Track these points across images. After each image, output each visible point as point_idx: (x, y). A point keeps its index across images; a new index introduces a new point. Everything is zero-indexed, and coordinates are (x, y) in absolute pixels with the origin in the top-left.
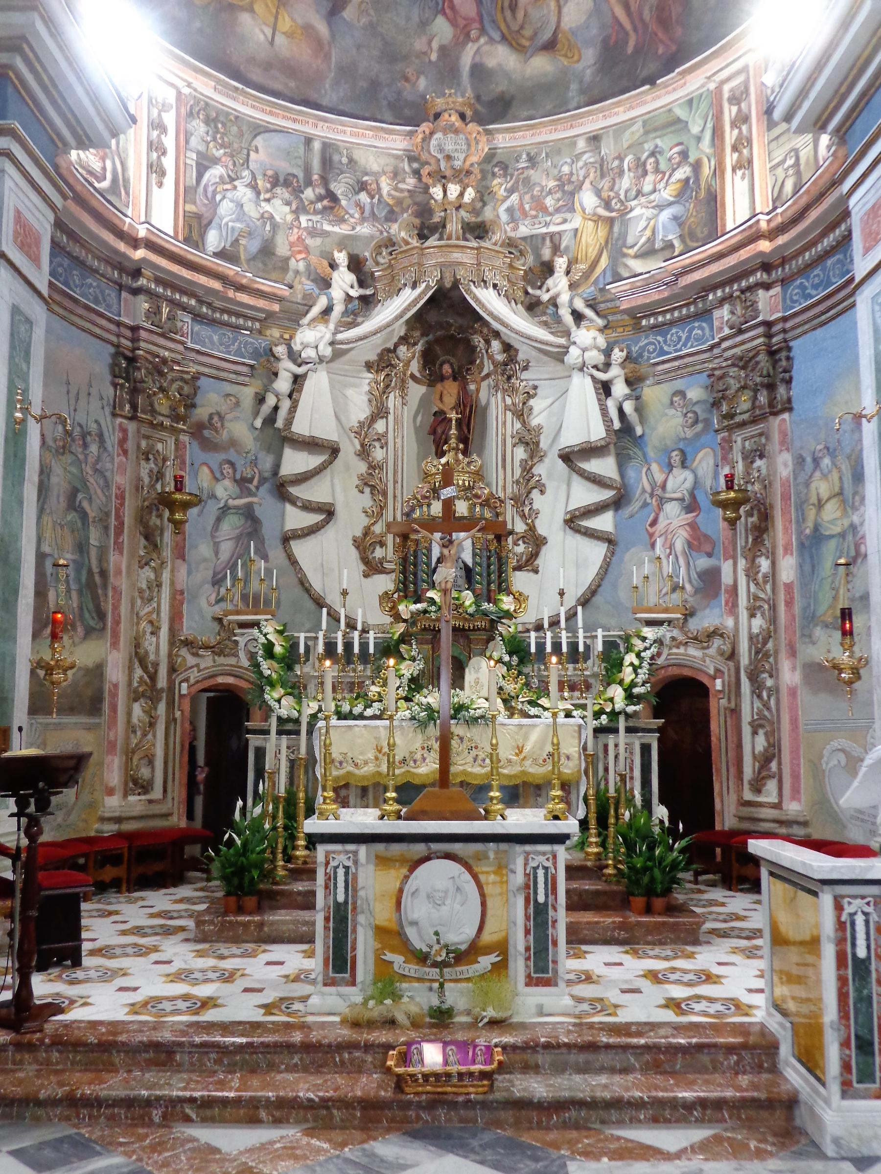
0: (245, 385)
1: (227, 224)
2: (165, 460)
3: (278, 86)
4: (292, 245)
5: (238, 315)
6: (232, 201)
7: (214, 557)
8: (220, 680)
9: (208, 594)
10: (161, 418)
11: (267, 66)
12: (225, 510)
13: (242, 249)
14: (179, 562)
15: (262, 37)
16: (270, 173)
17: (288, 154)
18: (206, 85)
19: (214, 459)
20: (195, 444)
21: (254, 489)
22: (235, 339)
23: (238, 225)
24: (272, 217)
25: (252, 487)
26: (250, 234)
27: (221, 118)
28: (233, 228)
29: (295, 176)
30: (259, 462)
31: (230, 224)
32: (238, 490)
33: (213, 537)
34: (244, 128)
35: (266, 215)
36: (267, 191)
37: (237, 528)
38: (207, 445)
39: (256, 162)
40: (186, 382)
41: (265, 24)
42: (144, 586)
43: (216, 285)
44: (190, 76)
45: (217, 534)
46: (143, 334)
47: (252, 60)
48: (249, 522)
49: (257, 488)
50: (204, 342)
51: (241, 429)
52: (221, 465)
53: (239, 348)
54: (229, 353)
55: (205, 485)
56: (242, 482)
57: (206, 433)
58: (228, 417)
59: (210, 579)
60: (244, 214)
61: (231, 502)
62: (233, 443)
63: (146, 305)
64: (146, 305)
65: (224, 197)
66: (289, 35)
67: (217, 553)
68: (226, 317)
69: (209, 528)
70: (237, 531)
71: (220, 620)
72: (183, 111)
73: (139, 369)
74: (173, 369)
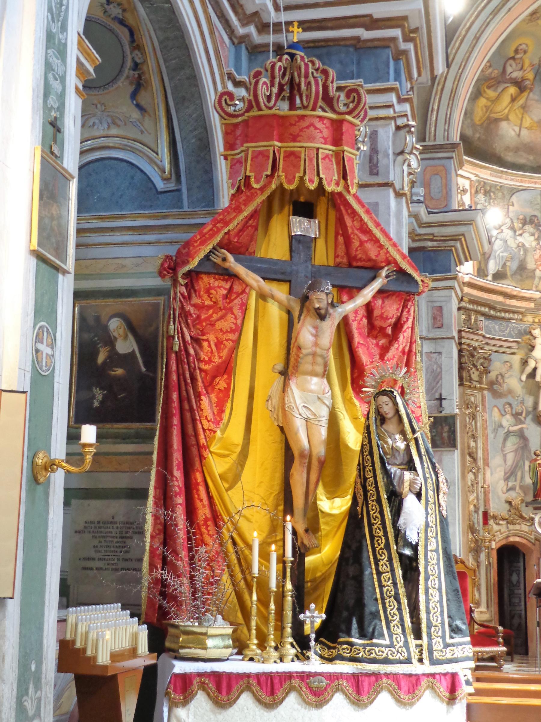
0: (514, 354)
1: (499, 255)
2: (476, 407)
3: (521, 161)
4: (536, 261)
5: (509, 312)
6: (501, 240)
7: (503, 464)
8: (512, 539)
9: (502, 485)
10: (475, 383)
11: (517, 150)
12: (508, 434)
13: (508, 268)
14: (486, 467)
15: (513, 133)
16: (521, 217)
17: (531, 203)
18: (486, 174)
19: (501, 402)
20: (490, 394)
21: (523, 419)
22: (507, 326)
23: (505, 254)
24: (524, 245)
25: (522, 418)
26: (512, 259)
27: (493, 190)
28: (502, 257)
29: (535, 216)
30: (525, 402)
31: (501, 254)
32: (514, 420)
33: (502, 451)
34: (505, 193)
35: (520, 245)
36: (521, 229)
37: (515, 445)
38: (496, 394)
39: (513, 212)
40: (485, 359)
41: (515, 125)
42: (469, 484)
43: (500, 299)
44: (478, 171)
45: (504, 449)
46: (463, 334)
47: (507, 149)
48: (522, 440)
49: (525, 418)
50: (491, 331)
51: (514, 382)
52: (504, 406)
53: (510, 331)
54: (504, 336)
55: (496, 419)
56: (516, 415)
57: (495, 387)
58: (506, 375)
59: (502, 477)
60: (508, 246)
61: (511, 429)
62: (510, 392)
63: (464, 317)
64: (464, 317)
65: (496, 239)
66: (529, 129)
67: (505, 461)
68: (503, 315)
69: (500, 445)
70: (515, 447)
71: (510, 503)
72: (473, 191)
73: (464, 356)
74: (479, 353)
